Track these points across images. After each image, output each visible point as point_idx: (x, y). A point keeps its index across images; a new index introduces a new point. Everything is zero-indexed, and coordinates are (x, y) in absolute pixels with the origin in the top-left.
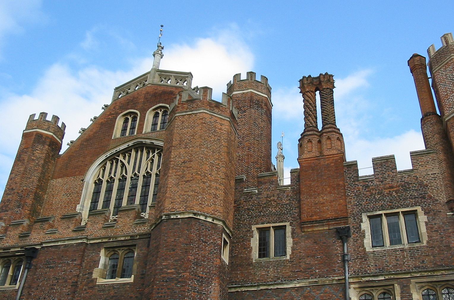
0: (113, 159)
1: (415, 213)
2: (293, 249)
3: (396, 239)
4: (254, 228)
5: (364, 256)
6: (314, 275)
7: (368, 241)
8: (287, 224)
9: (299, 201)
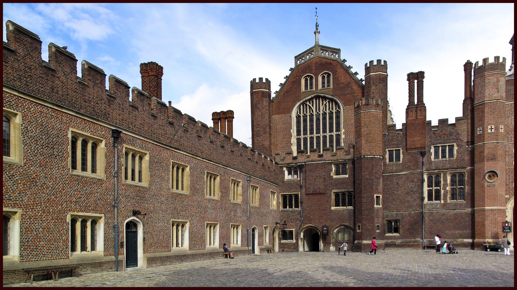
0: (303, 104)
1: (453, 145)
2: (403, 159)
3: (444, 156)
4: (387, 150)
5: (431, 162)
6: (411, 169)
7: (433, 157)
8: (401, 149)
9: (406, 139)
